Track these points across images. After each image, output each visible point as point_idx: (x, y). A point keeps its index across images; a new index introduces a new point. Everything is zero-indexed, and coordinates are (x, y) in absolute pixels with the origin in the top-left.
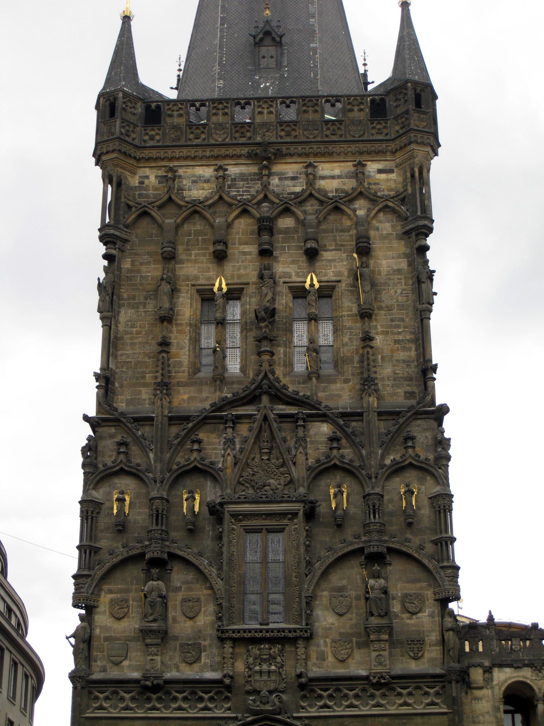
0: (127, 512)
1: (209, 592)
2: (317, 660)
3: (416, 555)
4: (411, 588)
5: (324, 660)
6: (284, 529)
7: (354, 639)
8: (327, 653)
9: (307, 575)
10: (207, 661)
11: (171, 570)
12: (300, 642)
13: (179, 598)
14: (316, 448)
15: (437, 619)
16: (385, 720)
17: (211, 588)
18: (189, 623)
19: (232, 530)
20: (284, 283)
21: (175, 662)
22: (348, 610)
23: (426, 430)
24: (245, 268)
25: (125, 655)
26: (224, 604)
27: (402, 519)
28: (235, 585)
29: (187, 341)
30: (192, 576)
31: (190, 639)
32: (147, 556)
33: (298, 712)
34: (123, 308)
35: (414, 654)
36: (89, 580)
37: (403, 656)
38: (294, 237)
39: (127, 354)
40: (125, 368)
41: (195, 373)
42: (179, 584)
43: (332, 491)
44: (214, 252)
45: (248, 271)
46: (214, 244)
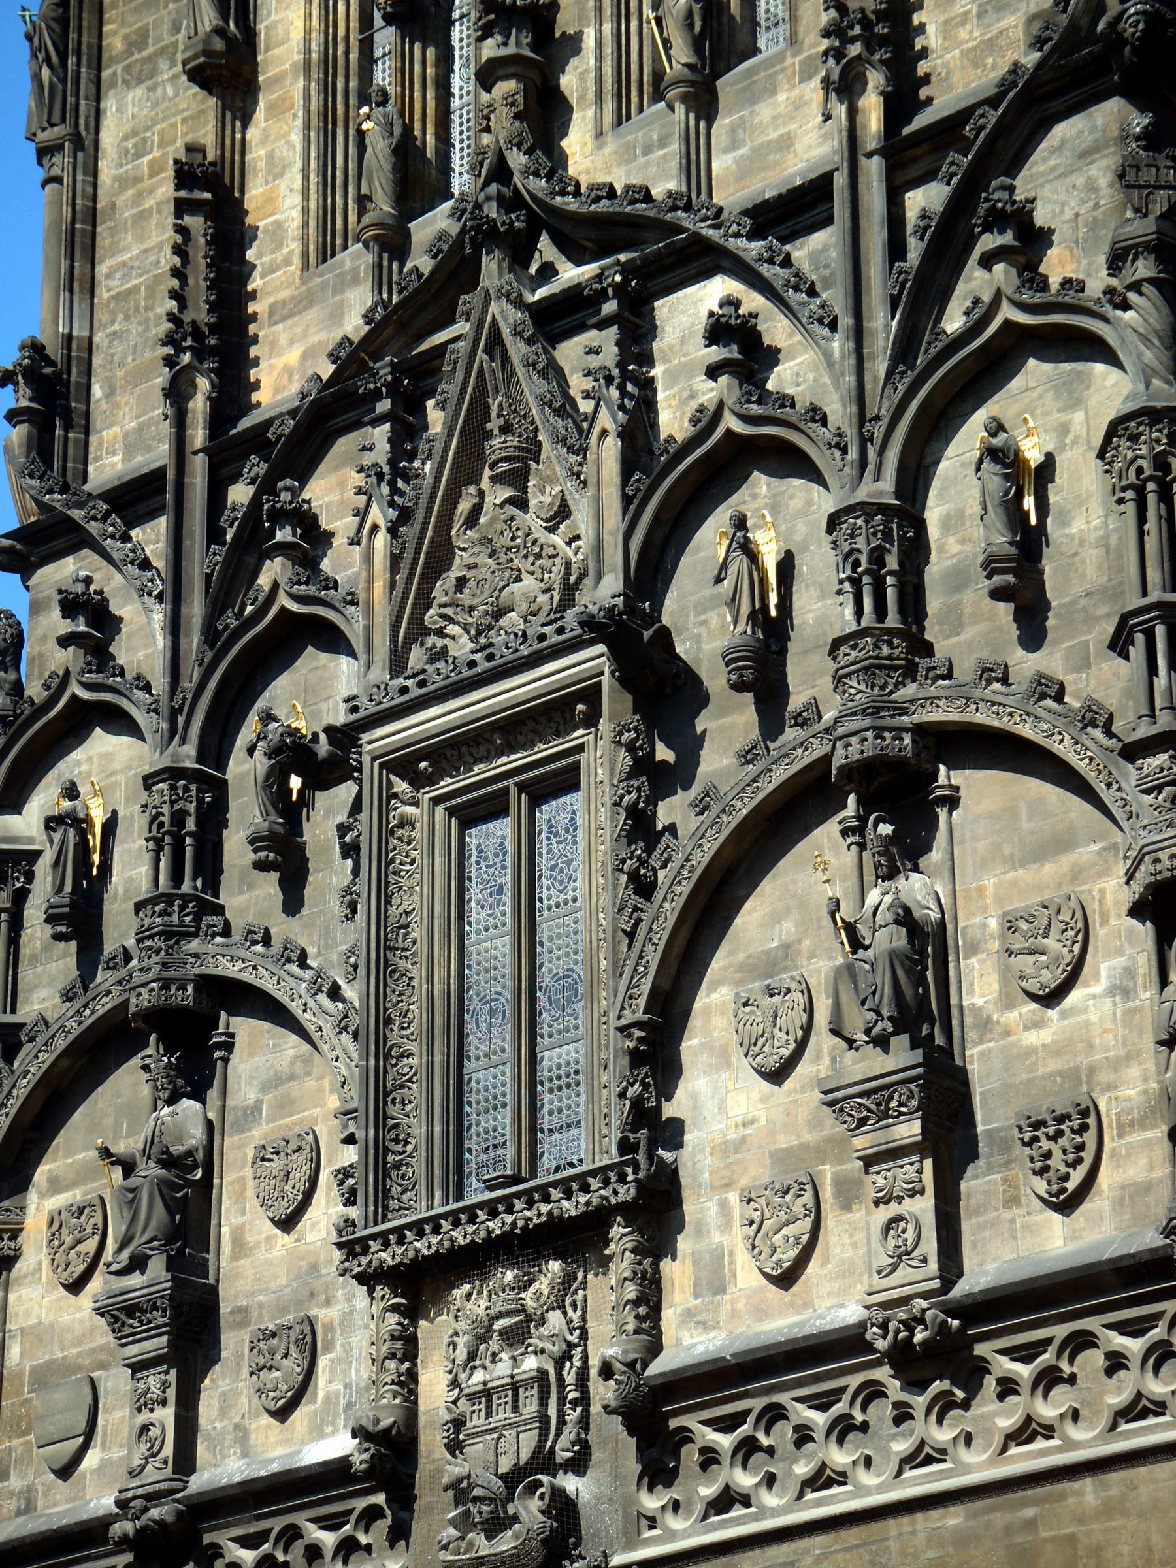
0: (96, 858)
2: (696, 1296)
3: (1026, 731)
5: (722, 1290)
6: (576, 766)
7: (827, 1173)
8: (731, 1254)
10: (338, 1386)
11: (229, 1047)
12: (616, 1231)
13: (251, 1153)
14: (685, 394)
15: (1147, 995)
16: (954, 1518)
18: (284, 1241)
19: (401, 825)
21: (237, 1420)
22: (801, 1047)
23: (1086, 155)
25: (82, 1426)
26: (360, 1135)
28: (412, 1047)
29: (297, 138)
30: (291, 1052)
31: (284, 1310)
33: (630, 1546)
34: (112, 93)
35: (1049, 1182)
37: (1013, 1201)
39: (124, 264)
40: (120, 317)
41: (326, 253)
42: (252, 1096)
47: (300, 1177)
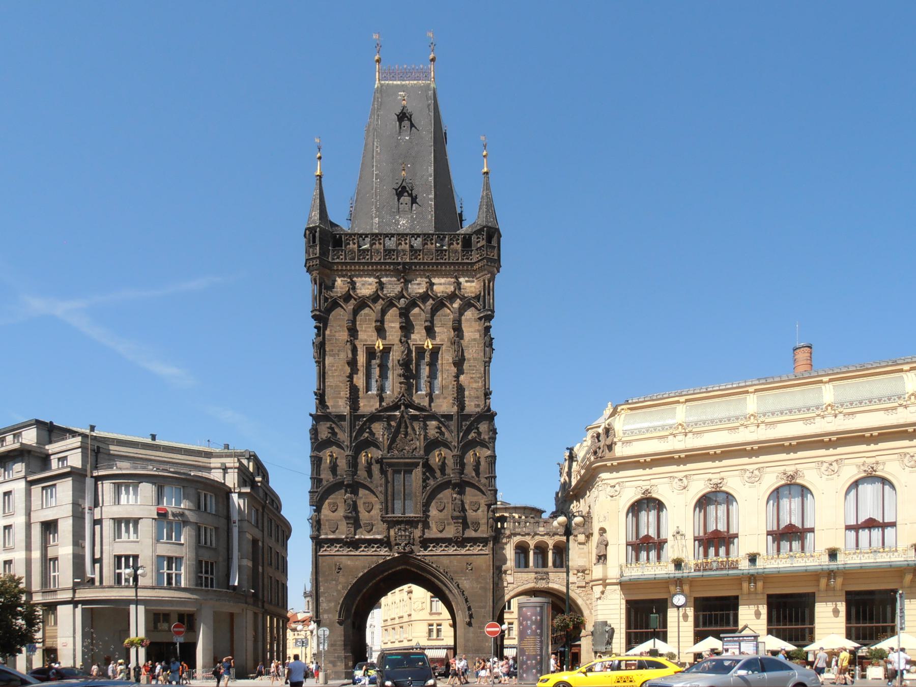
1: (377, 499)
3: (477, 484)
4: (474, 499)
9: (423, 493)
13: (362, 502)
17: (377, 497)
20: (413, 345)
24: (392, 335)
27: (471, 466)
32: (345, 483)
36: (317, 494)
38: (418, 319)
43: (437, 453)
44: (375, 326)
45: (393, 337)
46: (375, 321)
47: (370, 507)
